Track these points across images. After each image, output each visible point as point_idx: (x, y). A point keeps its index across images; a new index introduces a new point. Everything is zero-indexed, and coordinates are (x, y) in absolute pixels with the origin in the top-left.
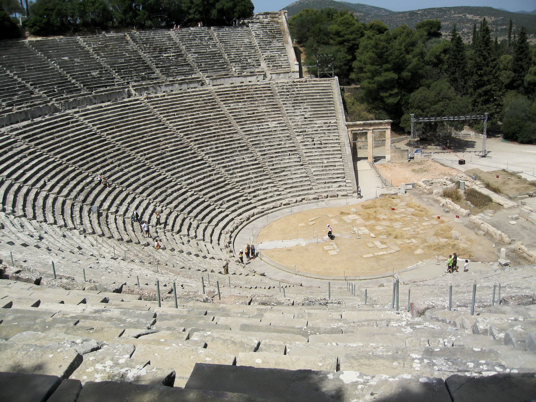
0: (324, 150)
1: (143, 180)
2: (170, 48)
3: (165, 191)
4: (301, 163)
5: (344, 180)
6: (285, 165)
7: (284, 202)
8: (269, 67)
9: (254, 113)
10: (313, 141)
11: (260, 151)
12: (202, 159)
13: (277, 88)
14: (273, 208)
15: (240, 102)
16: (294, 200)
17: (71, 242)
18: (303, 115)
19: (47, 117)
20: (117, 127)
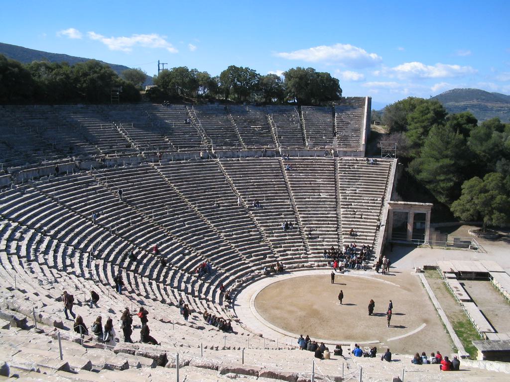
0: (362, 223)
2: (258, 121)
6: (321, 232)
8: (340, 145)
9: (311, 184)
10: (355, 214)
11: (303, 217)
12: (248, 217)
13: (339, 164)
15: (302, 173)
16: (316, 264)
18: (356, 190)
20: (186, 181)
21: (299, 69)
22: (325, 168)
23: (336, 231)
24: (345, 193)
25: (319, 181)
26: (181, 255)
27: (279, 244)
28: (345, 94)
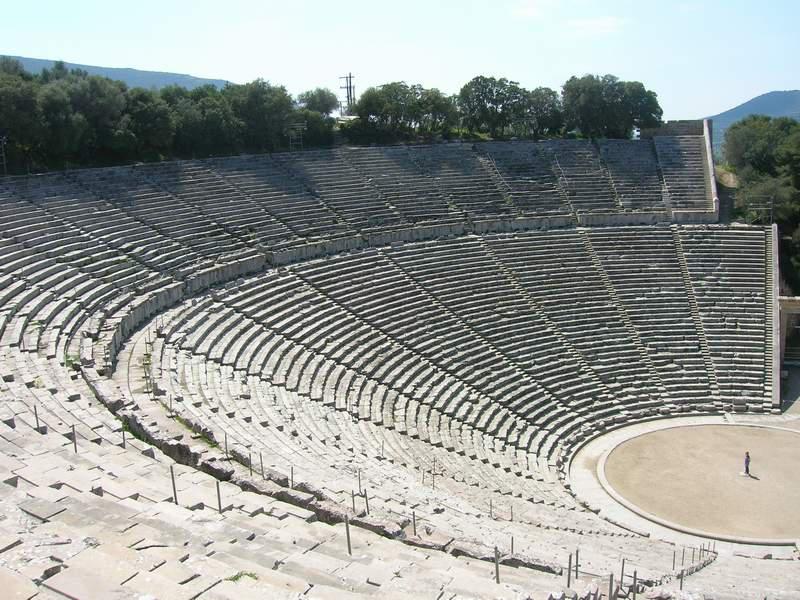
1: (460, 354)
3: (487, 373)
4: (700, 353)
5: (762, 385)
7: (661, 409)
9: (641, 272)
10: (724, 320)
11: (640, 329)
14: (645, 415)
16: (678, 407)
17: (332, 427)
19: (349, 255)
20: (440, 276)
21: (591, 77)
22: (660, 243)
23: (700, 350)
24: (700, 285)
25: (654, 267)
26: (467, 405)
27: (611, 375)
28: (665, 118)
